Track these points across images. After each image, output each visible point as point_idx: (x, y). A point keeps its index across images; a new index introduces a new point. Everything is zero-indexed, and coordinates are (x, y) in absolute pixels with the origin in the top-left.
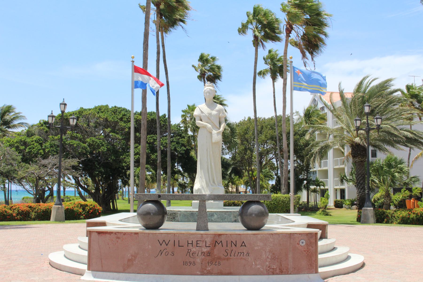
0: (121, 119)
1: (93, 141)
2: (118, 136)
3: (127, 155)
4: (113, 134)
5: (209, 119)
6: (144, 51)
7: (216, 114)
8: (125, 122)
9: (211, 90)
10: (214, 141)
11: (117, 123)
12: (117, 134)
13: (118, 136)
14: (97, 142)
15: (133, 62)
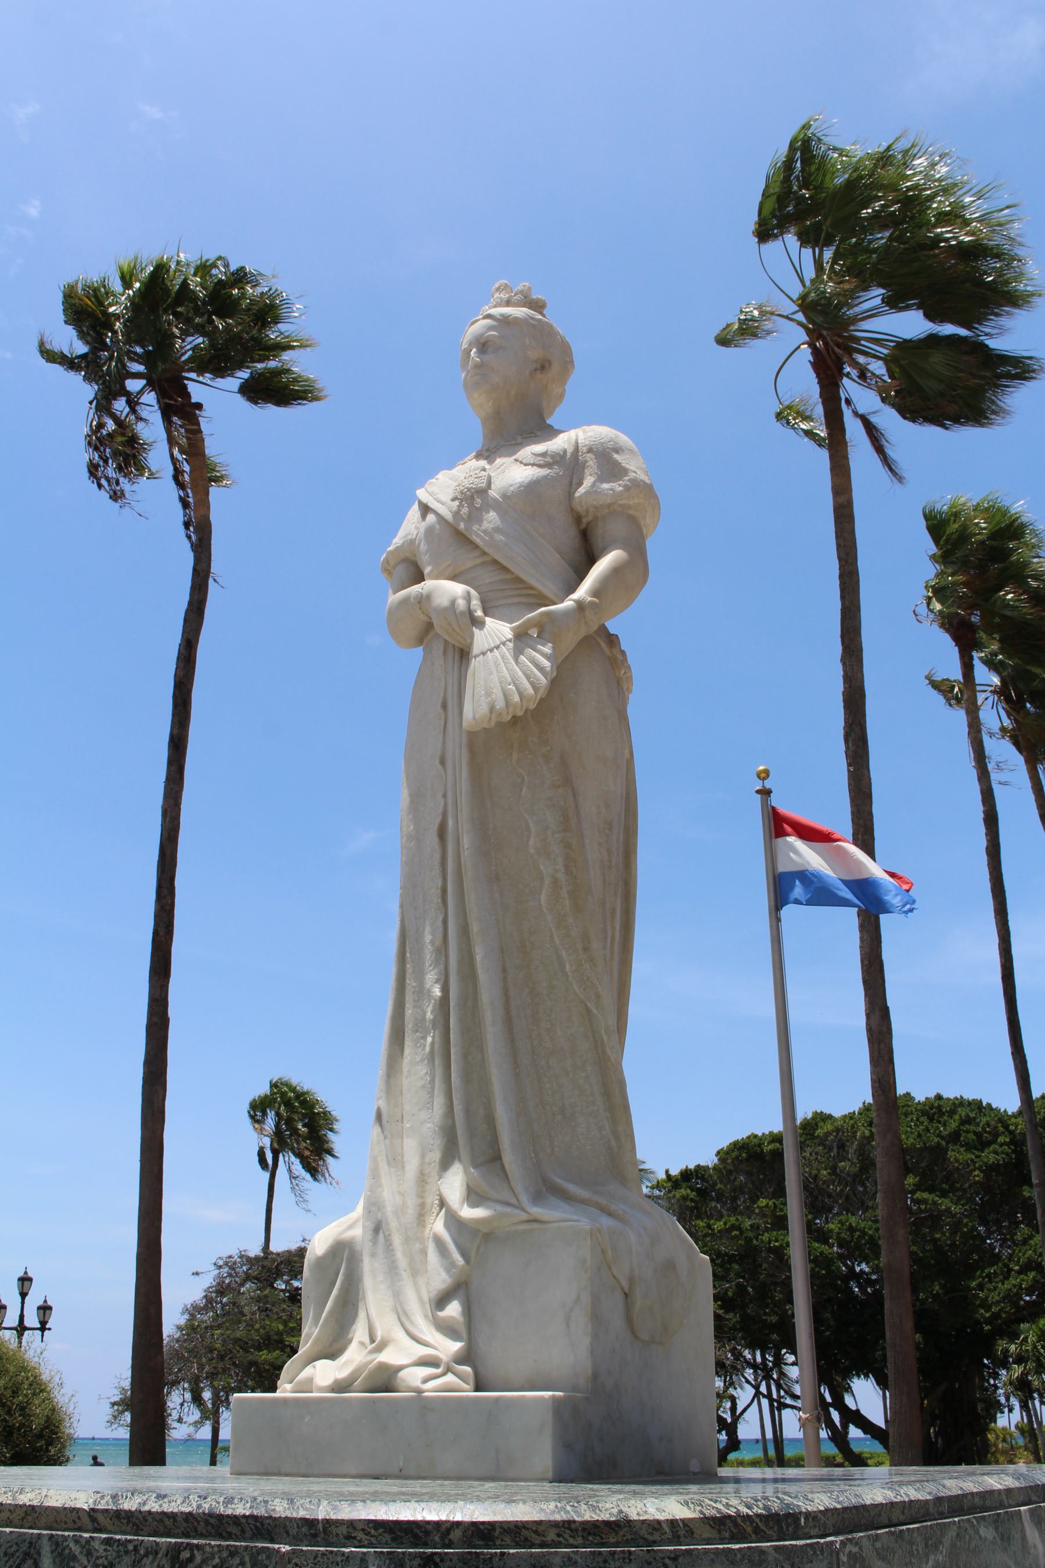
0: (954, 1137)
1: (851, 1229)
2: (945, 1203)
3: (989, 1275)
4: (926, 1195)
5: (462, 539)
6: (849, 765)
7: (531, 488)
8: (969, 1147)
9: (505, 321)
10: (475, 709)
11: (938, 1153)
12: (944, 1194)
13: (945, 1203)
14: (864, 1233)
15: (765, 793)
